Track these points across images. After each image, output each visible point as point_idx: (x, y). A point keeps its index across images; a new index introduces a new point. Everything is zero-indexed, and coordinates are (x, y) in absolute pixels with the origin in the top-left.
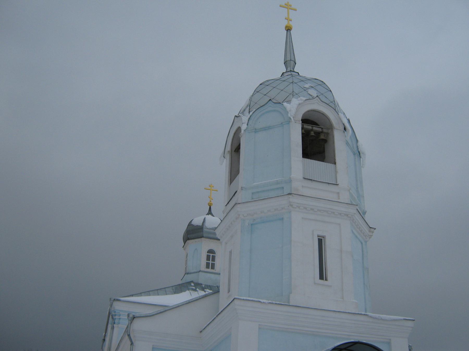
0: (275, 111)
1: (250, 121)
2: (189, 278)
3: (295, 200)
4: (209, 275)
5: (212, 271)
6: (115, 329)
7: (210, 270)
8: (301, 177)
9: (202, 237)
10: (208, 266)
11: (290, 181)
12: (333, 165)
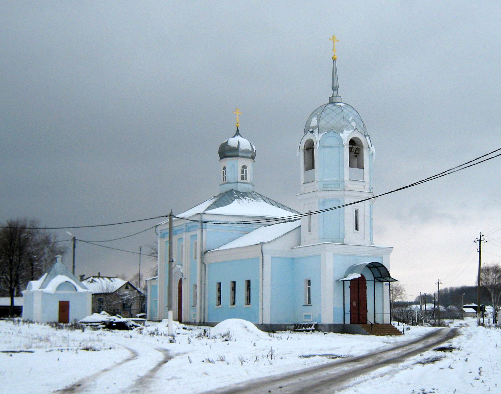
0: (334, 137)
1: (321, 141)
2: (229, 187)
3: (347, 193)
4: (244, 185)
5: (246, 181)
6: (204, 232)
7: (244, 181)
8: (348, 179)
9: (237, 156)
10: (242, 179)
11: (344, 181)
12: (362, 169)
